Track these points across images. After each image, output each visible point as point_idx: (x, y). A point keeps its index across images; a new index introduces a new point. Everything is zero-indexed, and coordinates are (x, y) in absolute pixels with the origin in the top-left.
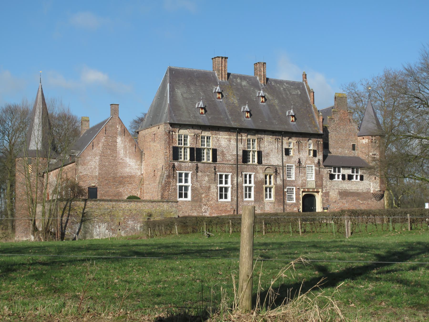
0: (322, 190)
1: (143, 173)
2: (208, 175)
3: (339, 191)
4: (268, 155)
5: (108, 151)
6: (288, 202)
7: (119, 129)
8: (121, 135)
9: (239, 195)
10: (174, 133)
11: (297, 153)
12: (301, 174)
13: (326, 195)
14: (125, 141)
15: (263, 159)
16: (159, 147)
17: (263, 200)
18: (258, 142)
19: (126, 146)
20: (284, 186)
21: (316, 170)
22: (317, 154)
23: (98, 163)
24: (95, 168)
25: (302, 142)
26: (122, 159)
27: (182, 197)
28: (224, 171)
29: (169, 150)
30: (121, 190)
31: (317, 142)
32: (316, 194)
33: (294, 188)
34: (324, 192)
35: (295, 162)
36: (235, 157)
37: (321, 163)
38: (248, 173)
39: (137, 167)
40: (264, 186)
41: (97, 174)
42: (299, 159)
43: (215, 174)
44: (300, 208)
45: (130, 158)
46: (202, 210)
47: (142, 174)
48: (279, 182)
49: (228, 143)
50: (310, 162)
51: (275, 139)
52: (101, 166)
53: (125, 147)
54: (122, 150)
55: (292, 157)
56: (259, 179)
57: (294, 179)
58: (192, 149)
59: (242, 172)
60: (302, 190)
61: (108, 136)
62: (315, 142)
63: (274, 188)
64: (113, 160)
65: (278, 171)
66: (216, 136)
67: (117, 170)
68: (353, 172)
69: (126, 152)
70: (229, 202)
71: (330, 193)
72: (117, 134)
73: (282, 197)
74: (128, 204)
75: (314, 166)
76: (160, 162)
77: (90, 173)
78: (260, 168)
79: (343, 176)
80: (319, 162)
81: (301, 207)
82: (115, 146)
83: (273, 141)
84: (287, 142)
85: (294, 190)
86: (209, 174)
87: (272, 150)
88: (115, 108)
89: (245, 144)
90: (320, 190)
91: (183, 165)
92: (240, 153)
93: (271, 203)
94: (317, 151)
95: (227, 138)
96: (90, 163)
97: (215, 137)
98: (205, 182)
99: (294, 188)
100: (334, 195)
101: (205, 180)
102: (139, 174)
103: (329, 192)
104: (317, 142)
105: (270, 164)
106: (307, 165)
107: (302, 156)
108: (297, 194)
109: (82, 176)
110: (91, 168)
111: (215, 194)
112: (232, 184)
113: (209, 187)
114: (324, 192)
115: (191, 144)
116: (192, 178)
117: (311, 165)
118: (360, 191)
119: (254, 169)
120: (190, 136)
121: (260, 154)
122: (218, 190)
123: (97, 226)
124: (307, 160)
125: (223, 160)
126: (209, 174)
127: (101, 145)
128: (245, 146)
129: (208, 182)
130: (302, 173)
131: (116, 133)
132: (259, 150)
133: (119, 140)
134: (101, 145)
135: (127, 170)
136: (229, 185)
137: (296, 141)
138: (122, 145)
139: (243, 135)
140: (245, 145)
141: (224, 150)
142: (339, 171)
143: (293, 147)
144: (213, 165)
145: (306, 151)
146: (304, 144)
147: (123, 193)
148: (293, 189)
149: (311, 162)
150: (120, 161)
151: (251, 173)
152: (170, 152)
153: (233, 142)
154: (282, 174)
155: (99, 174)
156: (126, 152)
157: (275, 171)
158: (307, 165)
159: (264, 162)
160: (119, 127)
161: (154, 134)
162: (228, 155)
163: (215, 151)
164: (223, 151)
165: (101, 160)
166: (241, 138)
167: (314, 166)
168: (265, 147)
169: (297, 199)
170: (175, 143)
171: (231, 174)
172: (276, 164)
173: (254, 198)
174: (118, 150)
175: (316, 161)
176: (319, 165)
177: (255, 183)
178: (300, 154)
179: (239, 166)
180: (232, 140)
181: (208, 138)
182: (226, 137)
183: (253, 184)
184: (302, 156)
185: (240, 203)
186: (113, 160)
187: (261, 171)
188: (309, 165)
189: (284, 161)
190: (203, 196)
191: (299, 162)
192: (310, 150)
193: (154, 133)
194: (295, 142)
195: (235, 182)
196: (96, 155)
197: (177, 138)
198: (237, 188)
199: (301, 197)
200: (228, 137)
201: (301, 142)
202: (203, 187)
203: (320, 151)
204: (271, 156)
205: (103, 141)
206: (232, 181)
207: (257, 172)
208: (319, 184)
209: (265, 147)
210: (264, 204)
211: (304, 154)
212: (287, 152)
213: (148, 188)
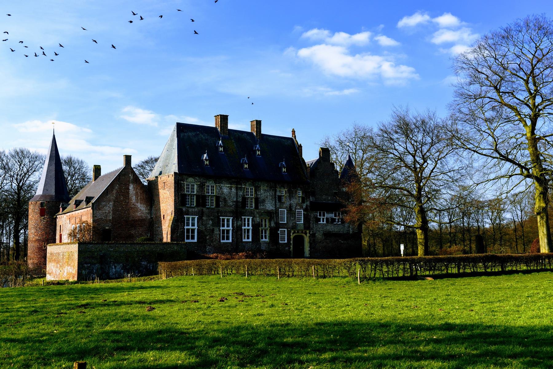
1: (152, 216)
2: (212, 219)
3: (324, 233)
4: (264, 201)
5: (121, 197)
7: (132, 178)
8: (133, 183)
10: (182, 182)
13: (313, 236)
14: (137, 189)
16: (169, 194)
17: (259, 241)
19: (137, 192)
21: (304, 214)
23: (112, 208)
24: (109, 212)
26: (133, 204)
27: (189, 239)
29: (178, 197)
30: (133, 232)
33: (286, 230)
34: (311, 233)
35: (287, 207)
37: (309, 208)
38: (247, 218)
39: (147, 211)
40: (260, 229)
41: (111, 218)
42: (290, 205)
45: (141, 203)
47: (152, 218)
48: (273, 225)
52: (115, 211)
53: (136, 194)
54: (134, 197)
56: (256, 222)
57: (286, 222)
58: (198, 196)
60: (292, 232)
61: (122, 184)
64: (125, 205)
67: (129, 214)
68: (335, 216)
69: (137, 198)
71: (317, 234)
72: (130, 182)
74: (141, 246)
76: (169, 208)
77: (104, 217)
79: (327, 219)
81: (292, 246)
82: (128, 193)
87: (267, 197)
88: (128, 159)
90: (308, 232)
91: (190, 210)
92: (240, 199)
93: (266, 243)
96: (105, 208)
97: (219, 186)
98: (209, 225)
100: (319, 236)
101: (209, 224)
102: (149, 217)
103: (315, 233)
106: (297, 210)
108: (289, 236)
109: (97, 219)
110: (106, 212)
112: (232, 227)
113: (213, 231)
114: (311, 233)
115: (197, 191)
116: (198, 222)
118: (341, 232)
119: (251, 214)
120: (196, 184)
122: (220, 232)
123: (113, 267)
124: (296, 205)
125: (225, 206)
127: (114, 192)
128: (244, 194)
129: (212, 225)
130: (292, 217)
131: (129, 181)
133: (131, 187)
134: (114, 192)
135: (139, 214)
136: (231, 228)
138: (134, 192)
142: (324, 216)
143: (285, 194)
147: (134, 235)
148: (285, 231)
150: (132, 206)
152: (178, 199)
153: (234, 190)
155: (113, 217)
156: (137, 198)
158: (297, 210)
160: (131, 175)
161: (164, 183)
163: (218, 198)
164: (225, 198)
165: (114, 205)
167: (302, 211)
168: (261, 194)
169: (289, 239)
170: (184, 191)
173: (252, 239)
174: (130, 196)
178: (291, 200)
180: (233, 188)
183: (250, 227)
186: (125, 205)
187: (258, 215)
188: (299, 210)
190: (208, 237)
193: (164, 181)
194: (286, 190)
195: (235, 225)
196: (110, 201)
197: (186, 186)
199: (292, 237)
202: (208, 229)
205: (116, 188)
206: (233, 224)
209: (261, 194)
210: (261, 244)
212: (280, 198)
213: (157, 231)
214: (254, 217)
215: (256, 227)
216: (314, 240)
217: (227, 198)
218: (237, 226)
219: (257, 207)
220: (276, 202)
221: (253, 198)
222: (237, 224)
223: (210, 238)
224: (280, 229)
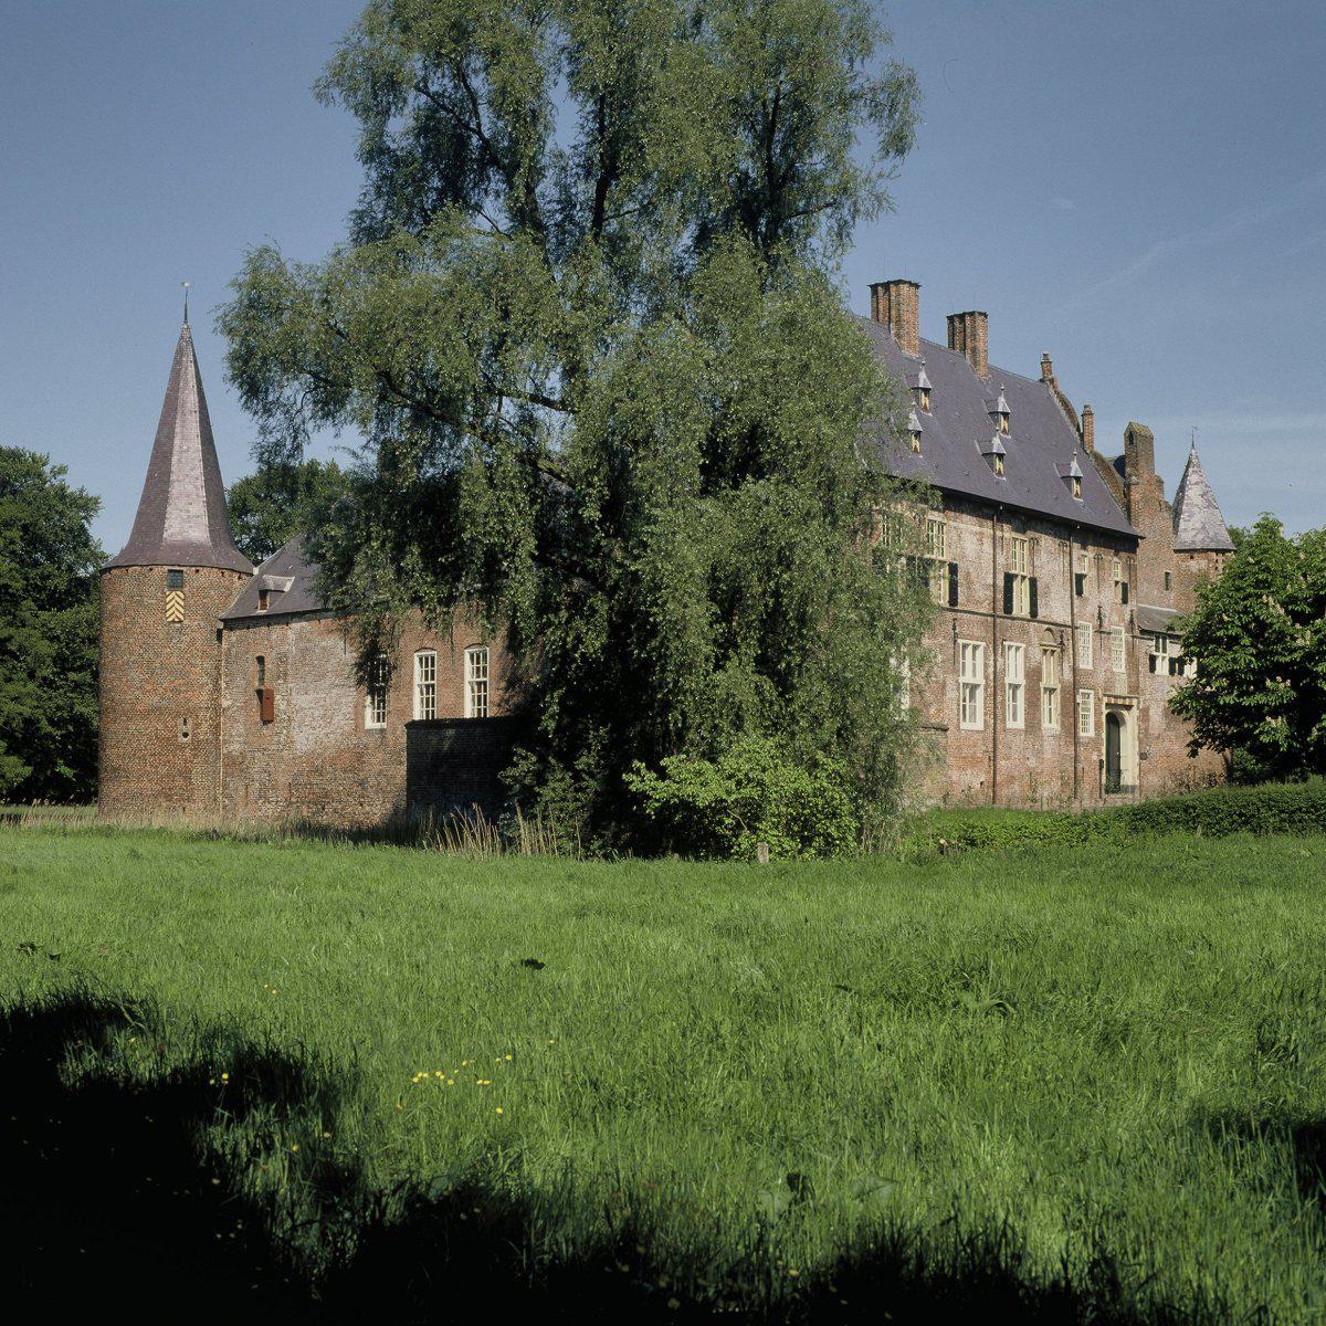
0: (1139, 703)
9: (999, 712)
20: (1075, 686)
32: (1125, 712)
36: (989, 593)
43: (955, 641)
48: (1068, 675)
55: (1087, 599)
65: (1065, 642)
66: (954, 524)
70: (978, 732)
71: (1151, 713)
73: (1072, 720)
75: (1123, 632)
78: (1035, 630)
86: (943, 641)
92: (1001, 582)
105: (1050, 620)
111: (955, 707)
112: (986, 678)
113: (944, 686)
121: (1033, 582)
136: (980, 679)
141: (971, 571)
144: (950, 615)
151: (1019, 644)
153: (987, 547)
154: (1071, 652)
159: (1042, 612)
162: (977, 586)
164: (968, 574)
169: (1098, 725)
175: (1128, 617)
179: (998, 620)
181: (942, 525)
185: (1000, 737)
189: (1075, 610)
195: (991, 670)
198: (996, 685)
207: (1029, 644)
208: (1135, 689)
214: (1029, 644)
215: (1034, 675)
216: (1146, 730)
217: (973, 575)
218: (995, 672)
219: (1034, 613)
220: (1072, 597)
222: (995, 666)
223: (939, 711)
224: (1081, 691)
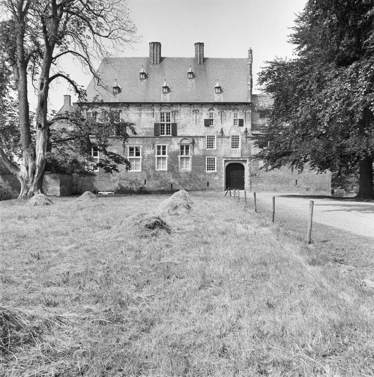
4: (184, 127)
6: (209, 171)
11: (220, 123)
12: (223, 144)
15: (178, 131)
18: (172, 114)
22: (244, 123)
25: (225, 112)
28: (134, 143)
31: (244, 111)
37: (249, 132)
44: (222, 177)
46: (111, 180)
49: (138, 117)
50: (235, 132)
51: (193, 111)
59: (154, 144)
62: (241, 111)
63: (191, 158)
80: (246, 131)
83: (190, 113)
84: (205, 114)
85: (216, 160)
89: (158, 118)
94: (244, 120)
95: (137, 113)
99: (216, 158)
104: (244, 111)
107: (226, 126)
117: (236, 135)
126: (117, 147)
132: (174, 122)
137: (218, 112)
139: (155, 109)
140: (157, 119)
145: (231, 121)
146: (227, 115)
149: (237, 131)
157: (192, 142)
166: (153, 112)
168: (181, 119)
171: (142, 146)
172: (194, 135)
176: (247, 135)
177: (169, 154)
178: (223, 124)
182: (136, 112)
184: (226, 126)
187: (176, 142)
191: (222, 132)
192: (234, 120)
200: (139, 112)
201: (224, 113)
203: (248, 120)
204: (188, 128)
209: (181, 119)
211: (227, 123)
221: (170, 124)
